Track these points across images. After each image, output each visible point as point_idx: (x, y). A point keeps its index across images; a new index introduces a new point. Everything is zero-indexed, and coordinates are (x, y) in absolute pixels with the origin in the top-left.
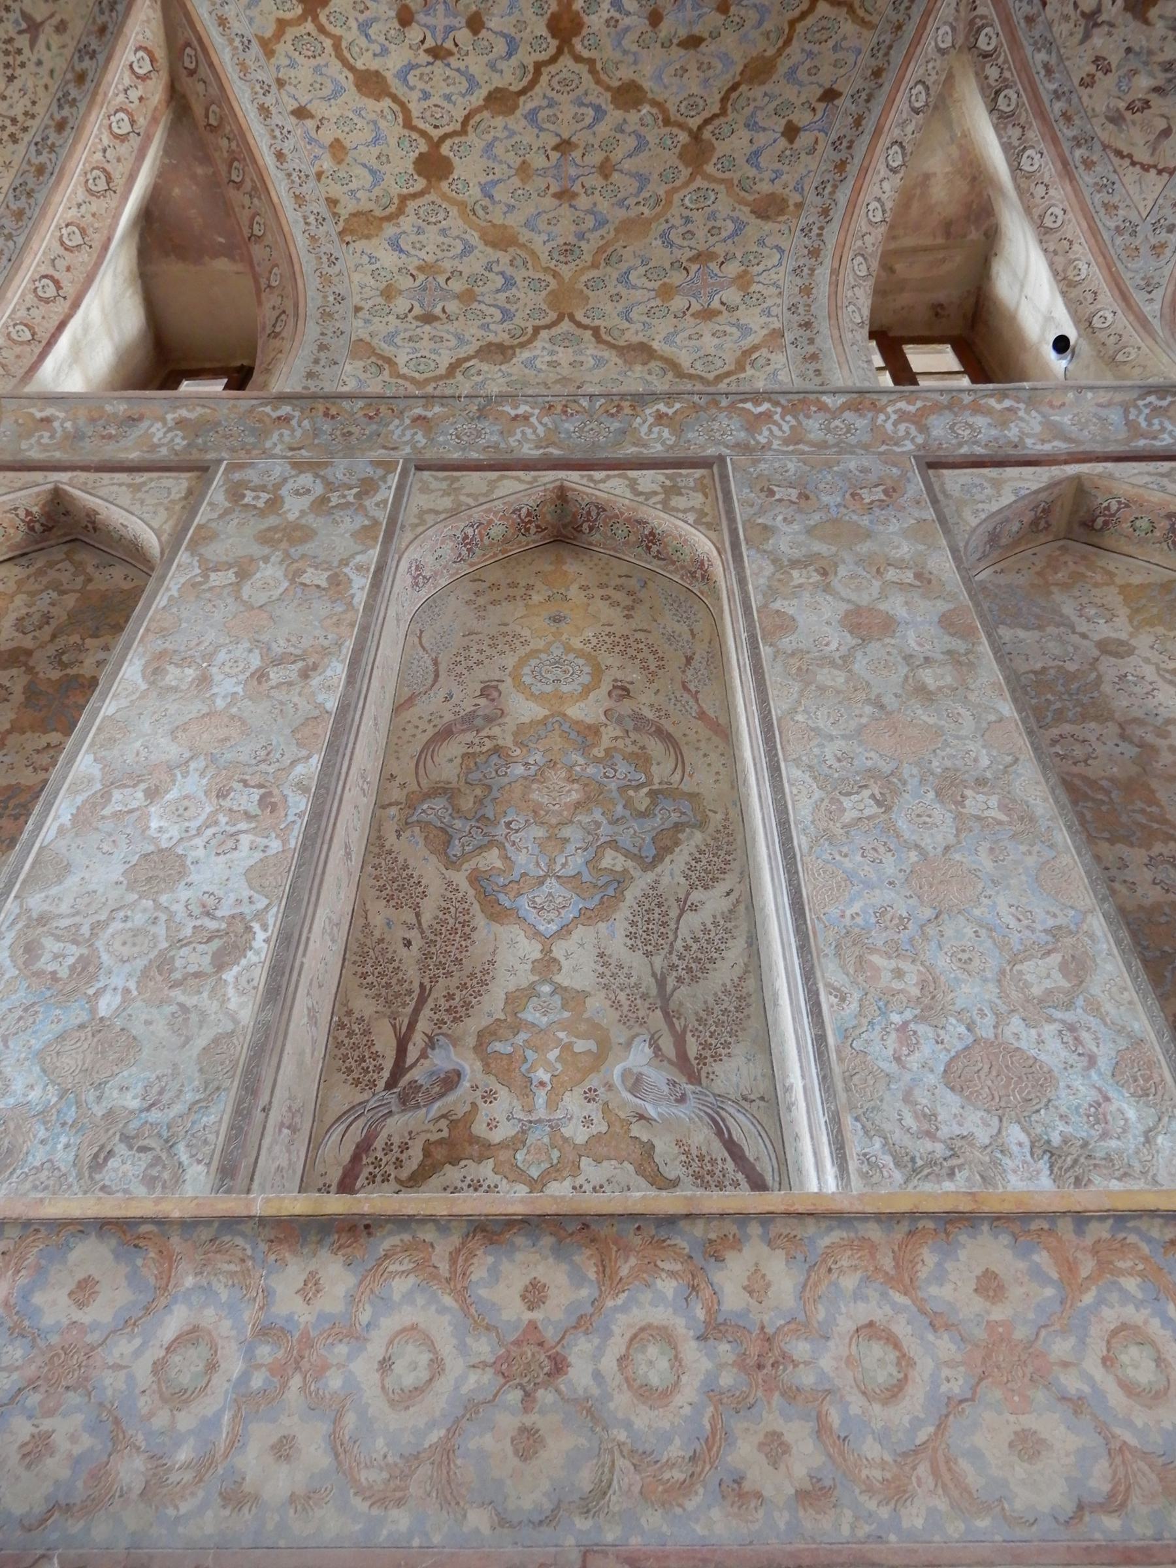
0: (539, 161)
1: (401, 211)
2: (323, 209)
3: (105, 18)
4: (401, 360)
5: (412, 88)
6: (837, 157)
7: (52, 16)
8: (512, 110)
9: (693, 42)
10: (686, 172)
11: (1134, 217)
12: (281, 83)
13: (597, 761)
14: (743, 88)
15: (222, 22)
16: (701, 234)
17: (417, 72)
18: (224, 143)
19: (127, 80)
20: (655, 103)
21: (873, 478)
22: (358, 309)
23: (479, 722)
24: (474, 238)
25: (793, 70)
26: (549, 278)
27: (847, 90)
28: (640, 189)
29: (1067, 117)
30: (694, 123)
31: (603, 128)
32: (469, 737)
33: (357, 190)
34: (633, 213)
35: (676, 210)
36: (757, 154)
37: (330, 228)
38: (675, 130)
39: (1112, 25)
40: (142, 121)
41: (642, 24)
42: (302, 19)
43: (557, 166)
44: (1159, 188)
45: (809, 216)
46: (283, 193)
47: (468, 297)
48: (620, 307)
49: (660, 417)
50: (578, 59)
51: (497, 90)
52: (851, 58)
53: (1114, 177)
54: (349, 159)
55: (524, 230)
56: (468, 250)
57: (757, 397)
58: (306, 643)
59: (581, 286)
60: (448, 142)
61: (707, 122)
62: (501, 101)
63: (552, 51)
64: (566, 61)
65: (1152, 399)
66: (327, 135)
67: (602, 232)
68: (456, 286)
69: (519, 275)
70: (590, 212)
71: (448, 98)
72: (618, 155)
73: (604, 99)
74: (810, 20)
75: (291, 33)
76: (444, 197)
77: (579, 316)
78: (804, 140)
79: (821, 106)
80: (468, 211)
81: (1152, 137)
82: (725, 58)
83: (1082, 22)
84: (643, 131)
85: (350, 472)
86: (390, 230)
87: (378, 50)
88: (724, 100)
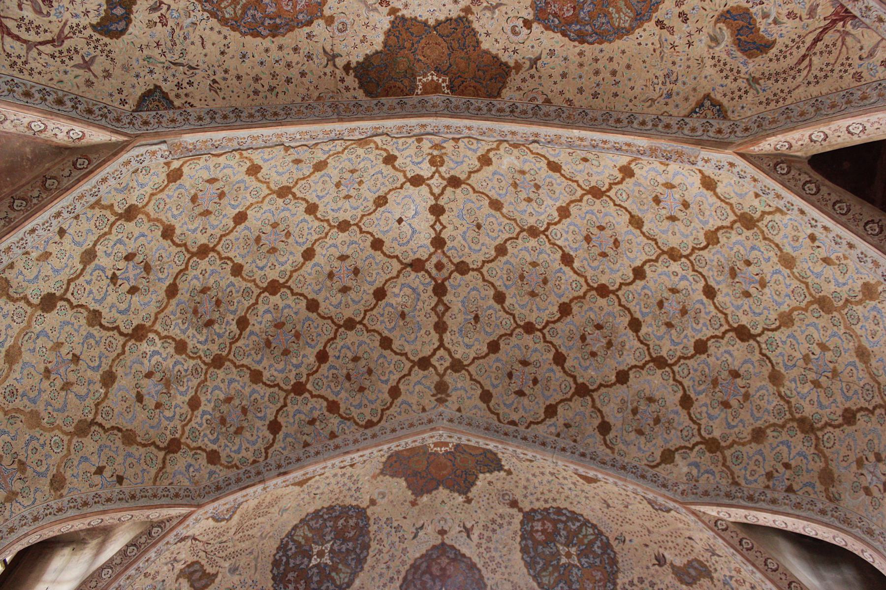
0: (64, 350)
2: (6, 261)
3: (97, 112)
5: (91, 274)
7: (95, 76)
8: (90, 324)
9: (140, 398)
10: (71, 429)
12: (77, 217)
14: (120, 434)
15: (104, 180)
16: (37, 456)
17: (101, 273)
18: (36, 193)
19: (65, 129)
20: (106, 394)
25: (130, 455)
28: (58, 410)
30: (99, 419)
31: (89, 373)
34: (44, 414)
35: (48, 435)
41: (146, 369)
42: (116, 214)
46: (9, 241)
50: (124, 346)
51: (100, 314)
52: (139, 481)
54: (41, 263)
55: (21, 364)
60: (65, 303)
61: (100, 425)
62: (95, 317)
63: (126, 331)
64: (122, 340)
66: (52, 248)
67: (28, 403)
70: (40, 391)
71: (91, 292)
72: (75, 388)
74: (155, 451)
75: (108, 213)
78: (97, 479)
79: (115, 478)
82: (134, 418)
84: (91, 395)
88: (113, 428)
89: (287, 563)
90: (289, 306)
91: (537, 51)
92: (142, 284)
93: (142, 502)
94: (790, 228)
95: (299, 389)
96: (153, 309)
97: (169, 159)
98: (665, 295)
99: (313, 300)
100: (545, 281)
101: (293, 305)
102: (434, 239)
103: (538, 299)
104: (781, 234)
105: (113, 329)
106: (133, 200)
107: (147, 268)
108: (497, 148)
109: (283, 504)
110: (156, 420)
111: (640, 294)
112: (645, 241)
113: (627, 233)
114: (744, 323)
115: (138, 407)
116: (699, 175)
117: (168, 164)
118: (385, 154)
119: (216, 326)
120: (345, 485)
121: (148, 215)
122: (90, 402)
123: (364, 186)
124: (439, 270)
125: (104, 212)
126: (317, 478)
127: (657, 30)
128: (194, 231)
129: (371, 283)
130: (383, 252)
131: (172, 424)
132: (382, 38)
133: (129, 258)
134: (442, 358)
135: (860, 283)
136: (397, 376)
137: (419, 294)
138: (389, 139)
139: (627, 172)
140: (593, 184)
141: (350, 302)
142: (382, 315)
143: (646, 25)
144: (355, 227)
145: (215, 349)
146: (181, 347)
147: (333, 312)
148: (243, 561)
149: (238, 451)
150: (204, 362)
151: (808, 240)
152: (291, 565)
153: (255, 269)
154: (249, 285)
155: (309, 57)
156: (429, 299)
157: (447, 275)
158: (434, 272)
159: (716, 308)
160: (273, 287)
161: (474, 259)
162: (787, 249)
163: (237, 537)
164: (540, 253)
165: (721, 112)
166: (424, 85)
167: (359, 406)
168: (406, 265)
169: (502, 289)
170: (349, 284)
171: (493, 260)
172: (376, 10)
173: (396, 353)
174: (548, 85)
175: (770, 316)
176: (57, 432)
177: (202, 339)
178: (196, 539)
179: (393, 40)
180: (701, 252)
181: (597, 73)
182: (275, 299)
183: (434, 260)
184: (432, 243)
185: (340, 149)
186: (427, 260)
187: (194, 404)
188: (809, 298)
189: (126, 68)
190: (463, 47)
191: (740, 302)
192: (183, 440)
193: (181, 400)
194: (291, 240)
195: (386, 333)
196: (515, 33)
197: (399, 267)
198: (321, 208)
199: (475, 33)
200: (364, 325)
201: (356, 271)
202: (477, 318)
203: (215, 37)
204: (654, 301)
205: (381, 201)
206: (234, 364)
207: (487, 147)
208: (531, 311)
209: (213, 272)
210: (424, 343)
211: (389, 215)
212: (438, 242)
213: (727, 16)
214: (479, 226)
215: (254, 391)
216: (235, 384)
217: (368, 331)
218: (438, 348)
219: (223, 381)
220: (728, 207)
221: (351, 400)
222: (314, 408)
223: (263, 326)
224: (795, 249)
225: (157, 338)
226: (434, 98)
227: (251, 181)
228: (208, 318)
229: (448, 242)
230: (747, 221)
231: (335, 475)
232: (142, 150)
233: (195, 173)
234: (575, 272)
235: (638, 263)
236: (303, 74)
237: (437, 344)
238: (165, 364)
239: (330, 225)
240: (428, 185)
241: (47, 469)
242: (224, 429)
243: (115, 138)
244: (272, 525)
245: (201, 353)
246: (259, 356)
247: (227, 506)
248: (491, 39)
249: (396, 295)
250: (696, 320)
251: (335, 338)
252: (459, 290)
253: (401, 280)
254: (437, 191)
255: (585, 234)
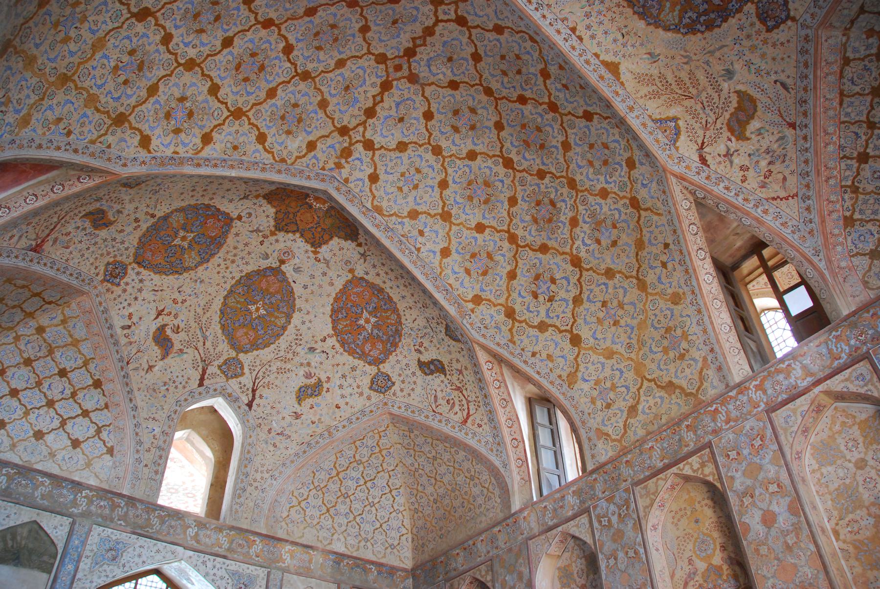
0: (601, 315)
1: (578, 365)
2: (558, 381)
4: (610, 433)
6: (683, 268)
11: (795, 223)
12: (523, 350)
13: (725, 581)
14: (640, 253)
15: (498, 344)
16: (662, 319)
20: (619, 272)
21: (755, 432)
22: (589, 414)
23: (692, 576)
24: (602, 359)
25: (650, 241)
26: (631, 362)
27: (669, 241)
29: (745, 200)
31: (610, 290)
32: (692, 583)
33: (563, 368)
34: (639, 320)
35: (650, 313)
36: (659, 278)
37: (565, 386)
38: (631, 279)
39: (737, 151)
40: (500, 378)
42: (513, 323)
43: (607, 313)
44: (796, 205)
45: (689, 297)
47: (613, 387)
48: (656, 362)
49: (687, 426)
50: (587, 270)
52: (663, 229)
53: (778, 210)
55: (613, 346)
56: (603, 365)
57: (710, 404)
58: (639, 582)
59: (641, 360)
61: (638, 271)
62: (577, 301)
63: (579, 272)
64: (585, 273)
65: (834, 333)
66: (544, 356)
68: (608, 384)
69: (621, 366)
71: (563, 312)
73: (604, 279)
75: (514, 330)
76: (585, 349)
77: (648, 377)
78: (670, 266)
79: (666, 251)
80: (593, 349)
81: (781, 184)
82: (627, 244)
83: (726, 159)
84: (622, 284)
85: (621, 498)
86: (579, 375)
87: (536, 313)
88: (637, 260)
89: (706, 12)
90: (511, 143)
91: (242, 202)
92: (547, 276)
93: (676, 222)
94: (86, 132)
95: (553, 107)
96: (559, 259)
97: (470, 312)
98: (210, 27)
99: (496, 128)
100: (317, 34)
101: (509, 141)
102: (387, 90)
103: (331, 22)
104: (93, 124)
105: (580, 283)
106: (502, 317)
107: (537, 277)
108: (298, 157)
109: (643, 66)
110: (624, 225)
111: (235, 24)
112: (212, 74)
113: (225, 78)
114: (139, 25)
115: (620, 243)
116: (151, 148)
117: (472, 311)
118: (374, 186)
119: (552, 196)
120: (600, 13)
121: (507, 299)
122: (626, 284)
123: (403, 169)
124: (401, 66)
125: (515, 333)
126: (601, 58)
127: (156, 213)
128: (503, 256)
129: (453, 96)
130: (429, 107)
131: (622, 209)
132: (331, 242)
133: (535, 296)
134: (445, 13)
135: (33, 121)
136: (488, 34)
137: (428, 60)
138: (363, 200)
139: (207, 139)
140: (237, 122)
141: (476, 101)
142: (463, 73)
143: (163, 214)
144: (432, 142)
145: (565, 190)
146: (574, 222)
147: (492, 109)
148: (718, 68)
149: (617, 142)
150: (577, 196)
151: (72, 129)
152: (706, 6)
153: (506, 186)
154: (517, 184)
155: (374, 266)
156: (423, 54)
157: (397, 59)
158: (405, 66)
159: (164, 28)
160: (508, 163)
161: (368, 62)
162: (89, 112)
163: (694, 91)
164: (308, 57)
165: (125, 185)
166: (324, 204)
167: (528, 53)
168: (423, 86)
169: (357, 34)
170: (467, 110)
171: (352, 57)
172: (324, 259)
173: (476, 46)
174: (244, 186)
175: (112, 41)
176: (647, 307)
177: (563, 204)
178: (703, 143)
179: (326, 237)
180: (165, 73)
181: (205, 190)
182: (513, 156)
183: (399, 74)
184: (392, 88)
185: (394, 218)
186: (404, 77)
187: (604, 194)
188: (76, 78)
189: (450, 353)
190: (287, 213)
191: (140, 42)
192: (629, 196)
193: (606, 208)
194: (473, 177)
195: (471, 62)
196: (250, 214)
197: (427, 88)
198: (439, 179)
199: (276, 219)
200: (480, 81)
201: (456, 113)
202: (395, 22)
203: (408, 316)
204: (223, 20)
205: (402, 147)
206: (568, 168)
207: (304, 160)
208: (342, 15)
209: (523, 221)
210: (448, 31)
211: (405, 131)
212: (386, 86)
213: (108, 224)
214: (347, 88)
215: (576, 144)
216: (580, 163)
217: (481, 76)
218: (442, 21)
219: (581, 174)
220: (133, 125)
221: (530, 62)
222: (559, 90)
223: (534, 157)
224: (85, 115)
225: (575, 246)
226: (321, 196)
227: (453, 249)
228: (550, 207)
229: (379, 83)
230: (120, 120)
231: (593, 37)
232: (473, 332)
233: (469, 288)
234: (286, 38)
235: (225, 51)
236: (383, 265)
237: (441, 24)
238: (588, 232)
239: (444, 161)
240: (364, 136)
241: (668, 309)
242: (610, 160)
243: (477, 348)
244: (673, 58)
245: (572, 202)
246: (553, 149)
247: (660, 136)
248: (267, 213)
249: (444, 74)
250: (187, 11)
251: (504, 98)
252: (395, 45)
253: (432, 79)
254: (361, 129)
255: (262, 75)
